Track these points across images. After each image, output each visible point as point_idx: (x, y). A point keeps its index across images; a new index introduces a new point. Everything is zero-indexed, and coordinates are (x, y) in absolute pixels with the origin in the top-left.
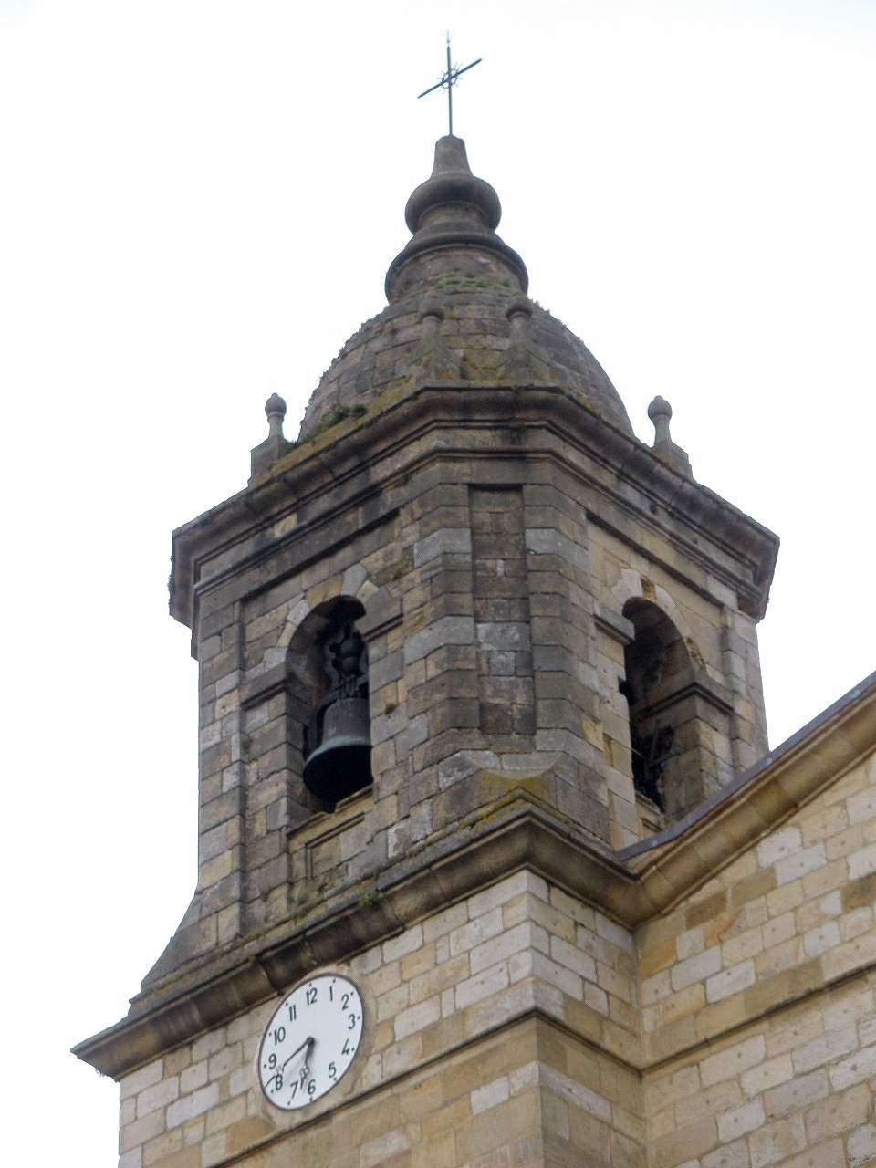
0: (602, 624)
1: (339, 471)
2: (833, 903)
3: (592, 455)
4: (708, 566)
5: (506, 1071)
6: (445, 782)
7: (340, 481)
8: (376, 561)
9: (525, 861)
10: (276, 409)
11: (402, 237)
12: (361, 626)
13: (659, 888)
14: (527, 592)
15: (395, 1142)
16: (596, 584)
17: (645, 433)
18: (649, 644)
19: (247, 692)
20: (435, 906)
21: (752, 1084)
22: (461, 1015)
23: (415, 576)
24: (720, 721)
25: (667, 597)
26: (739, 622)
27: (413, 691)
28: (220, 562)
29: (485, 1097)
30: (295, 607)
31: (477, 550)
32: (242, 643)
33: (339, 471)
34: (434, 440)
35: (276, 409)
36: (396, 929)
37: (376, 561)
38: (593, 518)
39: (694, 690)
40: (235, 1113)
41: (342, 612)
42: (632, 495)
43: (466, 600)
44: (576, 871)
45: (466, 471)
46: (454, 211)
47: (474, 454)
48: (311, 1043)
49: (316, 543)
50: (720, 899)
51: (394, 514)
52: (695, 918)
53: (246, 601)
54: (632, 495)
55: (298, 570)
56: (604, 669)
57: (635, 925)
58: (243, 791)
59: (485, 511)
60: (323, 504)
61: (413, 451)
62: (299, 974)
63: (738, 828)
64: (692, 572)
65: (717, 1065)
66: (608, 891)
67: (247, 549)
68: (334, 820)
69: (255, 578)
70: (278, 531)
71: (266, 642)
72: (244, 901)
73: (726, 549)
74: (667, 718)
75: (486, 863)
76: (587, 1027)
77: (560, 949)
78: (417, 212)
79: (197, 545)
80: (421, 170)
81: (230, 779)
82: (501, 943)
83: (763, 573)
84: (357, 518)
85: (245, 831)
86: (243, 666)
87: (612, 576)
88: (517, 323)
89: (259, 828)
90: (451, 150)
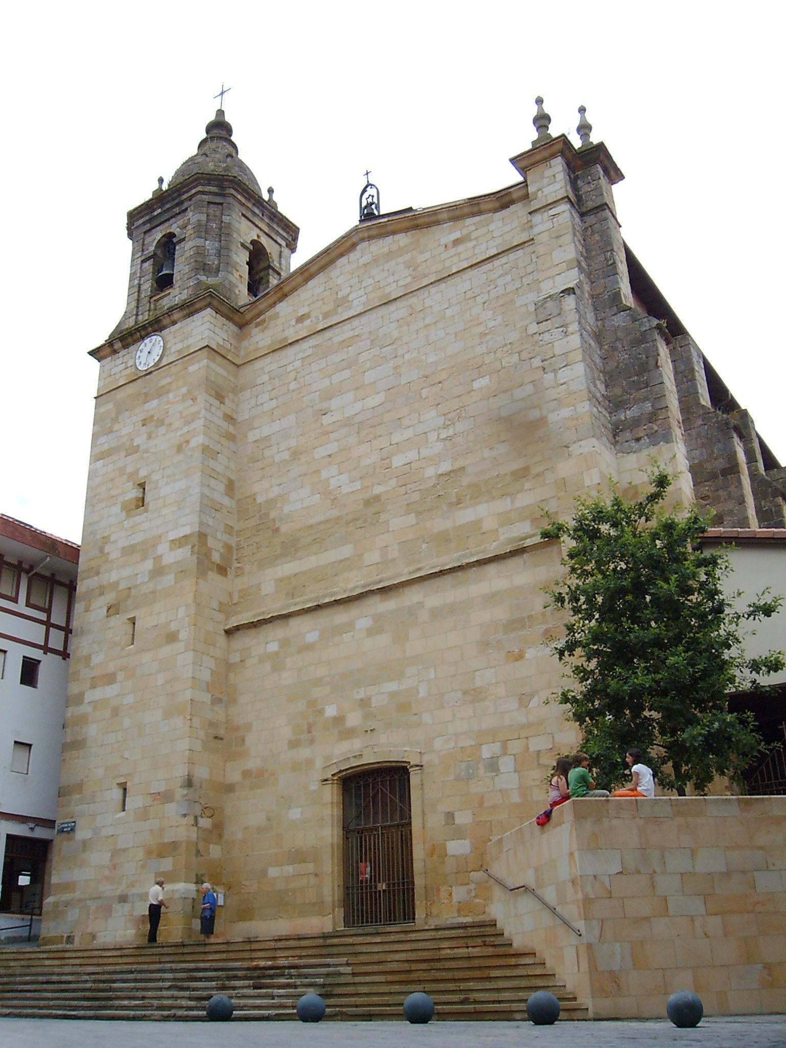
0: (243, 245)
2: (293, 322)
3: (246, 198)
5: (199, 362)
7: (173, 199)
8: (180, 222)
9: (209, 305)
10: (161, 180)
11: (204, 135)
12: (175, 240)
13: (248, 316)
14: (224, 233)
15: (169, 380)
16: (242, 234)
17: (266, 196)
18: (257, 254)
19: (143, 258)
21: (267, 369)
22: (189, 346)
23: (190, 227)
24: (276, 276)
25: (264, 240)
26: (286, 251)
28: (141, 220)
29: (192, 369)
30: (158, 235)
31: (208, 220)
32: (143, 244)
34: (200, 188)
35: (161, 180)
36: (174, 323)
37: (180, 222)
38: (243, 215)
39: (269, 267)
40: (128, 371)
41: (171, 235)
42: (257, 211)
43: (203, 234)
44: (224, 309)
45: (206, 198)
46: (219, 130)
47: (210, 193)
49: (166, 216)
50: (264, 320)
51: (186, 209)
52: (257, 325)
53: (145, 233)
54: (257, 211)
55: (160, 224)
56: (242, 258)
57: (241, 326)
58: (140, 285)
59: (212, 210)
60: (168, 206)
61: (193, 191)
62: (148, 335)
63: (271, 301)
64: (274, 237)
65: (258, 365)
66: (240, 320)
67: (147, 218)
68: (163, 294)
69: (148, 226)
70: (155, 213)
71: (150, 244)
72: (137, 315)
73: (283, 229)
74: (262, 274)
75: (198, 306)
76: (223, 353)
77: (217, 330)
78: (208, 130)
79: (133, 216)
80: (212, 117)
81: (136, 282)
82: (204, 327)
83: (295, 239)
84: (177, 210)
85: (139, 296)
86: (143, 251)
87: (246, 232)
88: (229, 159)
89: (143, 296)
90: (220, 113)
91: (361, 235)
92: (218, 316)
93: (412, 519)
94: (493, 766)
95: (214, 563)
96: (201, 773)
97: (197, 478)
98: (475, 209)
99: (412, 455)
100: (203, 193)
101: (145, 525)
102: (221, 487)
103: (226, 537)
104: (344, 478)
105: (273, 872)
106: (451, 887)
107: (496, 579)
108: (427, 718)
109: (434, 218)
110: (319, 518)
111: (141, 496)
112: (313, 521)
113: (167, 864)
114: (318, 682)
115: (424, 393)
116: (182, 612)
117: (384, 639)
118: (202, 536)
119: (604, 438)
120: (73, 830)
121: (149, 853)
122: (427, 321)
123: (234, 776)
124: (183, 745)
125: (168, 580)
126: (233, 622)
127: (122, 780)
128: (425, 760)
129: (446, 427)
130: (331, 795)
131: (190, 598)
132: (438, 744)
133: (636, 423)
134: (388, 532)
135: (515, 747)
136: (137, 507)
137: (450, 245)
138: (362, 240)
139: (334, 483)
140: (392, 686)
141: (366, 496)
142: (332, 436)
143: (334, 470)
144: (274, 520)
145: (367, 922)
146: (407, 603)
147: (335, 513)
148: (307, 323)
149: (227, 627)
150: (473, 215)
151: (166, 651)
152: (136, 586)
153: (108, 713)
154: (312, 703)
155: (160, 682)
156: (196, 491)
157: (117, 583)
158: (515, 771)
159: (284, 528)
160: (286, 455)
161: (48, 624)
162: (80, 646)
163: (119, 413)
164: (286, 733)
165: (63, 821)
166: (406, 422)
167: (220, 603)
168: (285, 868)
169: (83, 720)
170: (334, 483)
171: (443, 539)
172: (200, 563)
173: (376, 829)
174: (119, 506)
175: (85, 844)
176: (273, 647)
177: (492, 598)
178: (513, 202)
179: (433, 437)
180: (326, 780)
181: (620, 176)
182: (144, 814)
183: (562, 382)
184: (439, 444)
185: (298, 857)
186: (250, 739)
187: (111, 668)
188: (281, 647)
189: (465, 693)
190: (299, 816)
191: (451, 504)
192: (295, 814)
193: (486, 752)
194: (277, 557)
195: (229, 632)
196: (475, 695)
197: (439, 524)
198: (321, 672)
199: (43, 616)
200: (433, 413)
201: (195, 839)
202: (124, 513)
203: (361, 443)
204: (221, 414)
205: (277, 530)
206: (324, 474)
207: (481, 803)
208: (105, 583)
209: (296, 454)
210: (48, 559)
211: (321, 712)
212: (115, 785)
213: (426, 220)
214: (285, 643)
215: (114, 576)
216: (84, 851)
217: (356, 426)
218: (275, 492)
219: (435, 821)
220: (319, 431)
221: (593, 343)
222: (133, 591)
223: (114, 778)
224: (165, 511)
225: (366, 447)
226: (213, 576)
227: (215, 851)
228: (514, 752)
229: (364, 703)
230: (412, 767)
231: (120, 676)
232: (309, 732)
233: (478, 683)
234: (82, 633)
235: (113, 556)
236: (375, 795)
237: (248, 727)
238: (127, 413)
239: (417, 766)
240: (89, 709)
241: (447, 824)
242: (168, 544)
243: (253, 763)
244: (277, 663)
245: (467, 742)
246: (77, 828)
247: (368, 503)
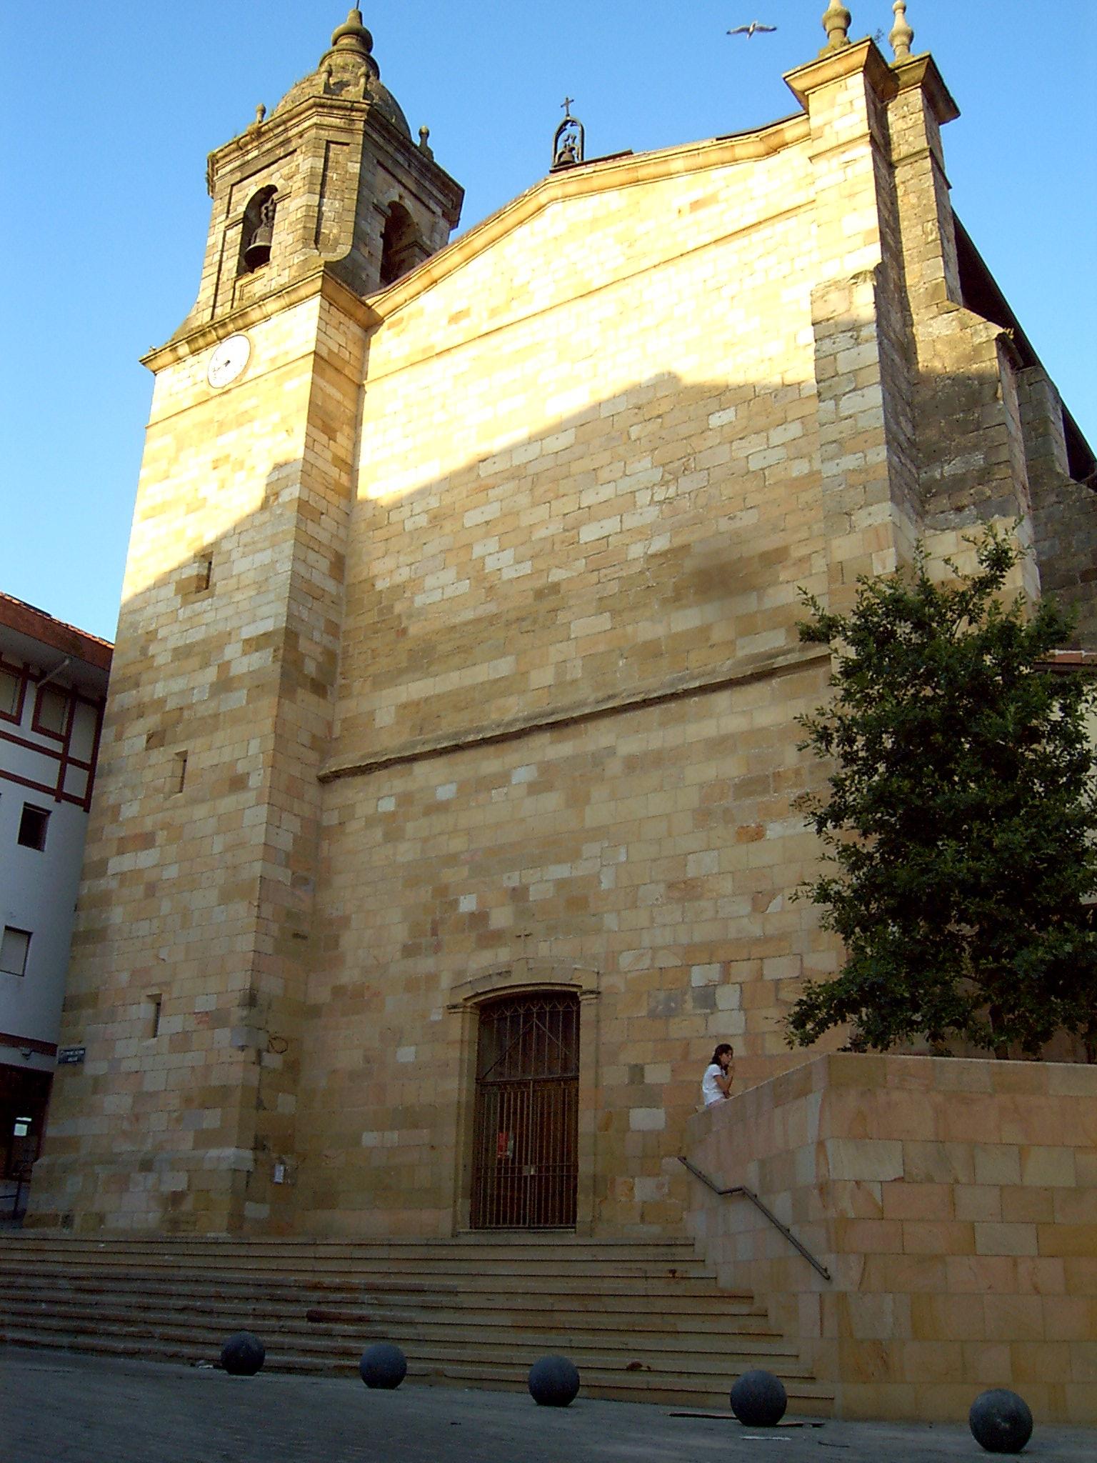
0: (376, 207)
1: (276, 132)
4: (431, 195)
6: (296, 261)
8: (285, 171)
12: (275, 196)
17: (417, 140)
19: (228, 222)
23: (299, 177)
25: (409, 204)
26: (443, 223)
27: (290, 224)
30: (252, 188)
33: (276, 132)
36: (267, 318)
41: (271, 189)
42: (401, 159)
47: (332, 127)
49: (265, 161)
50: (402, 320)
54: (401, 159)
60: (269, 146)
67: (238, 163)
68: (254, 276)
70: (249, 157)
72: (214, 307)
74: (404, 255)
76: (338, 364)
77: (331, 331)
83: (458, 206)
84: (281, 152)
92: (333, 310)
93: (604, 621)
94: (707, 998)
95: (306, 676)
96: (271, 986)
97: (288, 548)
99: (611, 525)
100: (318, 126)
101: (211, 614)
102: (324, 565)
103: (326, 640)
104: (508, 555)
105: (369, 1139)
106: (633, 1177)
107: (729, 715)
108: (610, 921)
110: (469, 615)
111: (205, 572)
112: (457, 620)
113: (212, 1119)
114: (451, 860)
115: (635, 432)
116: (254, 746)
117: (552, 801)
118: (290, 636)
119: (907, 505)
120: (81, 1060)
121: (188, 1101)
123: (321, 995)
124: (246, 944)
125: (238, 698)
126: (332, 766)
127: (156, 991)
128: (605, 982)
129: (664, 483)
130: (461, 1028)
131: (268, 725)
132: (626, 960)
133: (957, 483)
134: (569, 639)
135: (742, 971)
136: (198, 590)
137: (686, 209)
139: (491, 564)
140: (561, 871)
141: (539, 583)
142: (492, 493)
143: (493, 544)
144: (399, 616)
145: (504, 1222)
146: (591, 747)
147: (492, 608)
148: (464, 323)
149: (322, 773)
151: (228, 803)
152: (190, 706)
153: (140, 890)
155: (217, 848)
156: (285, 567)
157: (163, 701)
158: (741, 1008)
159: (413, 630)
160: (423, 521)
161: (64, 759)
162: (110, 791)
163: (180, 449)
164: (400, 933)
165: (66, 1047)
166: (604, 475)
167: (314, 736)
168: (387, 1134)
169: (104, 900)
170: (491, 564)
171: (651, 651)
172: (284, 674)
173: (526, 1085)
174: (173, 587)
176: (388, 805)
177: (719, 746)
180: (454, 1007)
181: (955, 113)
182: (182, 1042)
183: (846, 414)
184: (651, 508)
185: (409, 1118)
186: (348, 939)
187: (149, 824)
188: (398, 805)
189: (671, 886)
190: (411, 1058)
191: (665, 602)
192: (406, 1054)
193: (698, 976)
194: (401, 672)
195: (324, 780)
196: (686, 890)
198: (457, 844)
199: (57, 747)
200: (647, 462)
201: (256, 1083)
202: (179, 599)
203: (535, 504)
204: (329, 456)
206: (478, 551)
208: (146, 699)
210: (67, 662)
212: (143, 998)
214: (405, 799)
215: (160, 690)
216: (95, 1092)
217: (530, 479)
218: (404, 574)
219: (615, 1076)
220: (474, 485)
221: (897, 359)
222: (186, 714)
223: (144, 987)
224: (238, 597)
225: (542, 511)
226: (304, 695)
227: (286, 1104)
228: (739, 980)
229: (518, 894)
230: (584, 993)
231: (161, 836)
233: (691, 872)
234: (110, 772)
235: (160, 661)
236: (528, 1029)
237: (345, 921)
239: (592, 992)
240: (114, 884)
241: (632, 1082)
242: (239, 646)
243: (349, 975)
244: (392, 828)
246: (87, 1058)
247: (539, 595)
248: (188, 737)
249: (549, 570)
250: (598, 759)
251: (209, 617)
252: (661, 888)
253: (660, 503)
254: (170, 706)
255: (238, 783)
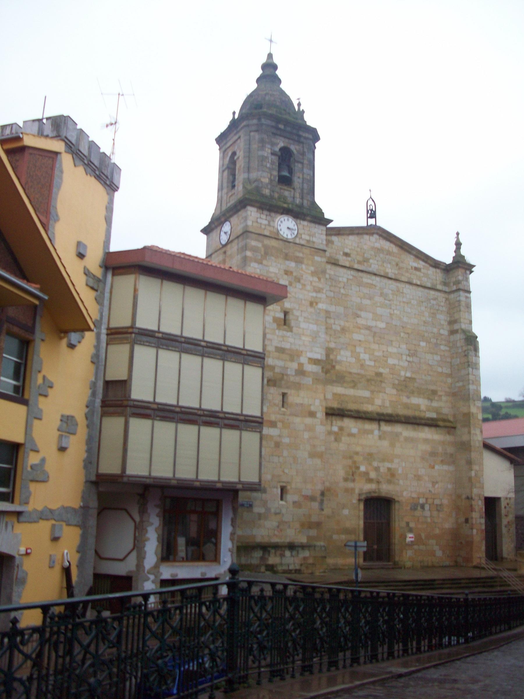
20: (311, 221)
22: (314, 242)
48: (288, 228)
91: (379, 232)
94: (423, 507)
98: (425, 260)
105: (335, 537)
108: (401, 482)
109: (410, 250)
114: (357, 453)
120: (251, 506)
121: (302, 525)
122: (405, 300)
125: (308, 381)
127: (284, 484)
129: (409, 355)
132: (405, 494)
135: (430, 501)
138: (377, 234)
140: (389, 465)
144: (332, 360)
147: (362, 372)
150: (423, 261)
154: (355, 462)
159: (338, 367)
160: (339, 328)
164: (341, 473)
171: (406, 406)
175: (260, 515)
176: (335, 429)
177: (426, 441)
178: (438, 268)
179: (404, 357)
185: (347, 531)
189: (415, 476)
193: (422, 501)
196: (418, 478)
197: (405, 400)
198: (359, 449)
205: (334, 367)
207: (418, 520)
209: (343, 330)
211: (358, 468)
212: (279, 487)
213: (407, 248)
214: (341, 429)
223: (280, 482)
229: (377, 469)
231: (279, 425)
232: (353, 475)
238: (273, 258)
245: (414, 495)
248: (288, 388)
249: (379, 367)
250: (398, 435)
251: (291, 340)
252: (413, 476)
253: (409, 362)
254: (277, 370)
255: (312, 414)
